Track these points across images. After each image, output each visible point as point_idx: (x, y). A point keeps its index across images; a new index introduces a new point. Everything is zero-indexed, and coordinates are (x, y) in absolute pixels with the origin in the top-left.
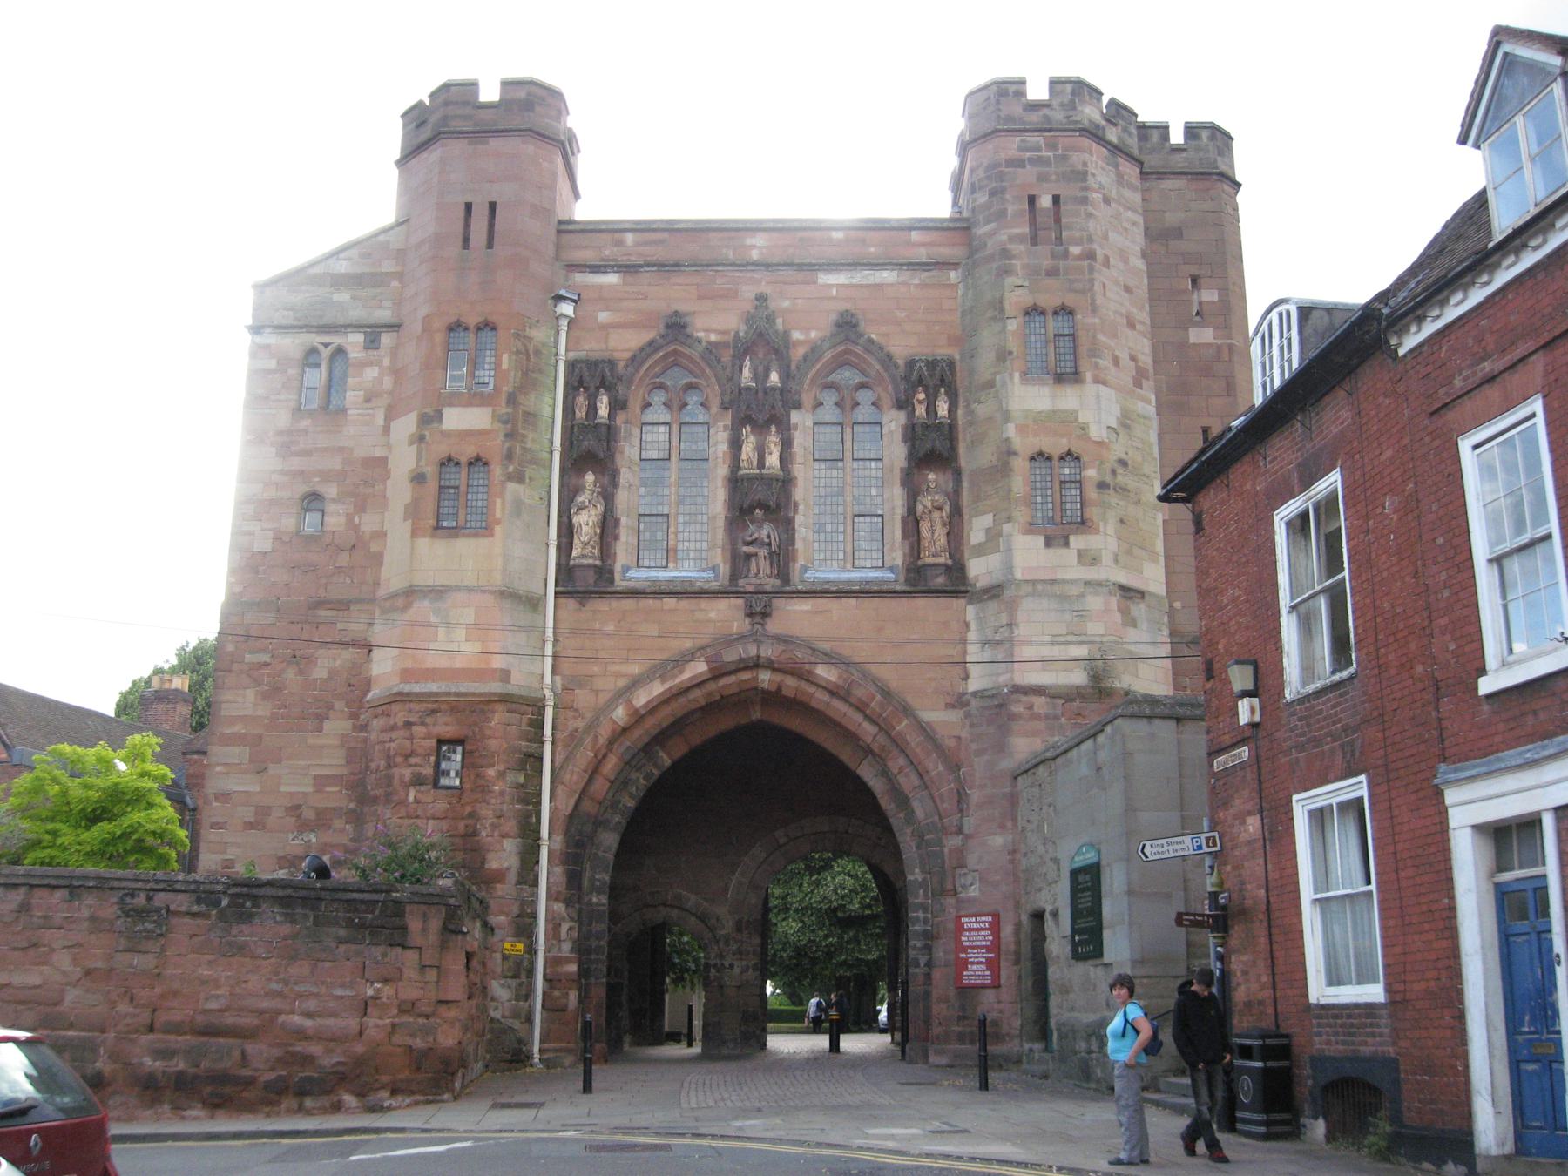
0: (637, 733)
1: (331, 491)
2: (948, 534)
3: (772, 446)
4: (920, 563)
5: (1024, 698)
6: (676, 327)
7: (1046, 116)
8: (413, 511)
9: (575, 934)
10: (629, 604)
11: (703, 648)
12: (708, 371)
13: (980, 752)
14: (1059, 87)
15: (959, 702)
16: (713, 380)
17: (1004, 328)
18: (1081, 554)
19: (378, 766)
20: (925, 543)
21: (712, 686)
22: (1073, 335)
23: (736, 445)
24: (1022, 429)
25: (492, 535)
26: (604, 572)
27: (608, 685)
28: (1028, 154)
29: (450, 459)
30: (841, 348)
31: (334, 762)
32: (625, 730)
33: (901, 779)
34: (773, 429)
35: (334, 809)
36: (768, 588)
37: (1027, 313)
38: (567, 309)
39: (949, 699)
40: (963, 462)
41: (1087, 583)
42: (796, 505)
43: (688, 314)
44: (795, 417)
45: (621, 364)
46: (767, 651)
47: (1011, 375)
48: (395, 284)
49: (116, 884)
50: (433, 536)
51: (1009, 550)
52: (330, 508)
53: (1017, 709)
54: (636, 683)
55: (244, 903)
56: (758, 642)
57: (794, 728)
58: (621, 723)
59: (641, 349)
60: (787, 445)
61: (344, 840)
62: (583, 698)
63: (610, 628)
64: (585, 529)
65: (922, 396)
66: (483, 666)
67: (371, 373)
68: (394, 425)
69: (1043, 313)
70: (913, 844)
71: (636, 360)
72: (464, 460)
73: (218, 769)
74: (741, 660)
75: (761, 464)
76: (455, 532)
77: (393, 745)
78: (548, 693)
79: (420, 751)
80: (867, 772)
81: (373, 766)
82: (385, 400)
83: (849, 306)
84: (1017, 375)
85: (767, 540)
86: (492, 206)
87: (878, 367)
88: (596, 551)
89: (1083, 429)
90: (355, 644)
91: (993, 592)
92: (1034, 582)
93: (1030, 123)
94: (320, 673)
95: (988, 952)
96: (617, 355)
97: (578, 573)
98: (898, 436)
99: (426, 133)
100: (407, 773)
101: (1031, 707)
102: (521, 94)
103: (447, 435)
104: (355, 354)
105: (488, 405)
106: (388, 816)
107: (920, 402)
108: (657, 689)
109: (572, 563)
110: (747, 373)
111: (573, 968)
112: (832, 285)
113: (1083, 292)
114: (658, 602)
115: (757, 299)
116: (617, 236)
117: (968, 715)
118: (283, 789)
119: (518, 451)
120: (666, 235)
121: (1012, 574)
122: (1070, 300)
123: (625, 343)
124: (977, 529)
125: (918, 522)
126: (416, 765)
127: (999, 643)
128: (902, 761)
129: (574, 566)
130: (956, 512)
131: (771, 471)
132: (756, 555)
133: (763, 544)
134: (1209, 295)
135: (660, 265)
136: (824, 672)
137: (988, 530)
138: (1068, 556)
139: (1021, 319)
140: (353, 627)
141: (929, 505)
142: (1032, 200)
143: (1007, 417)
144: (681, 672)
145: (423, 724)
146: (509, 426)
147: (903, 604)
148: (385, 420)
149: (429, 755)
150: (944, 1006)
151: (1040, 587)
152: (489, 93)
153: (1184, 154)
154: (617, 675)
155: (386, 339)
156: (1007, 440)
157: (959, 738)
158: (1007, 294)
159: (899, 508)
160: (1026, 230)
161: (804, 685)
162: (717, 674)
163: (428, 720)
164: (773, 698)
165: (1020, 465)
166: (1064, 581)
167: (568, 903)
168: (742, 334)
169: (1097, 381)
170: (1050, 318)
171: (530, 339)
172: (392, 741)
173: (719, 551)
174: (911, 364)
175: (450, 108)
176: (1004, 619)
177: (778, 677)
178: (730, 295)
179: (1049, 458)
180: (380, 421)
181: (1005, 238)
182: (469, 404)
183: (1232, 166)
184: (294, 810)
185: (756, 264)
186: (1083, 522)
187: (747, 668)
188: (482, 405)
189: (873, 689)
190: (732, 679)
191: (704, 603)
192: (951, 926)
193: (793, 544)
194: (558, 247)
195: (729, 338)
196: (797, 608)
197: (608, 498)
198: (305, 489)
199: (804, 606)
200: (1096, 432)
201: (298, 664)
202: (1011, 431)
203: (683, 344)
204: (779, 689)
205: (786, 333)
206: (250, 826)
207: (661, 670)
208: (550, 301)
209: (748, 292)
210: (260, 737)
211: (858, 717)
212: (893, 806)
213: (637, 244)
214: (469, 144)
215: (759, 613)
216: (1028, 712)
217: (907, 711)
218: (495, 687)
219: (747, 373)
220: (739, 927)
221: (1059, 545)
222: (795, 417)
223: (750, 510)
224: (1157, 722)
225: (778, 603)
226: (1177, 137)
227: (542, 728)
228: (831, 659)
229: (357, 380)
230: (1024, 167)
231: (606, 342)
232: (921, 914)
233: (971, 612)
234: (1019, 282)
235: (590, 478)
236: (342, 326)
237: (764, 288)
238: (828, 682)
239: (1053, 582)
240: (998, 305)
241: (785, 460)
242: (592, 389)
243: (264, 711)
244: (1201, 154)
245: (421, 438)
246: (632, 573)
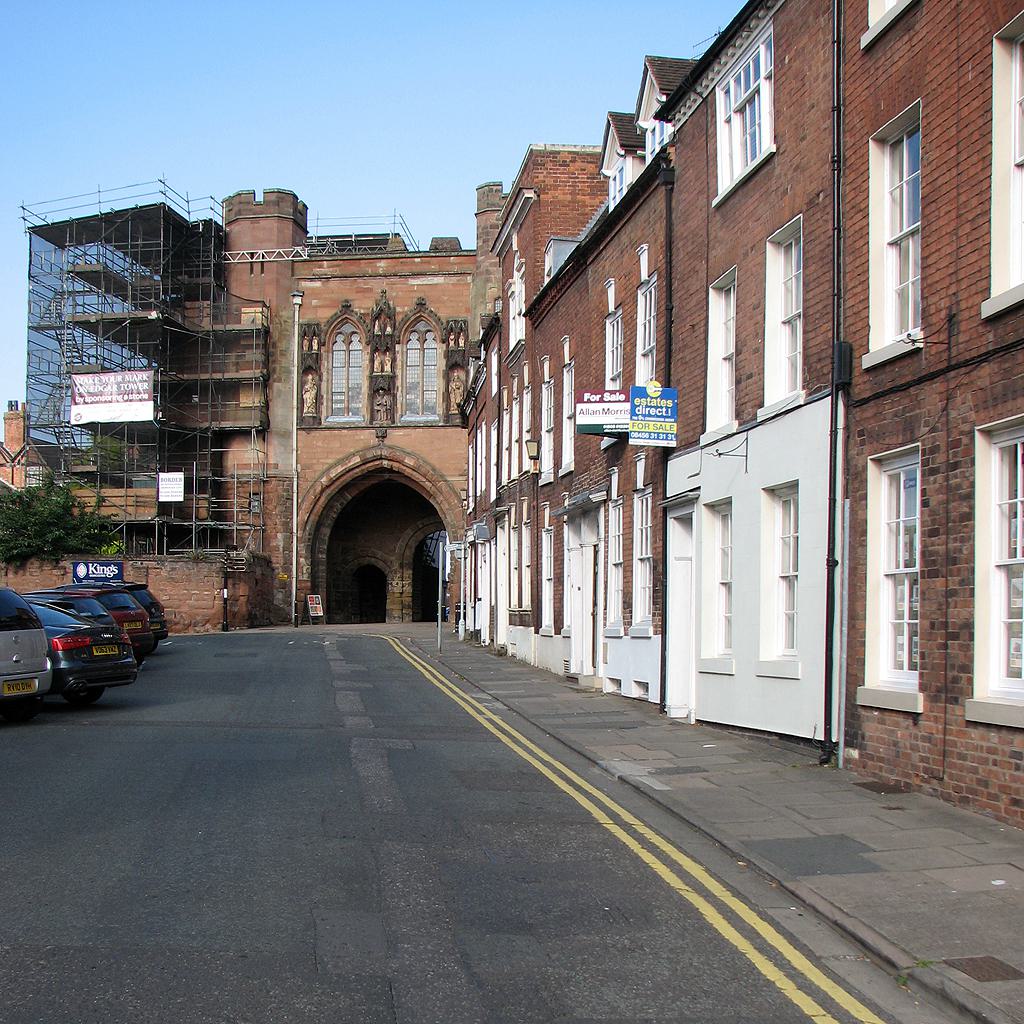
0: (332, 487)
6: (347, 307)
9: (310, 571)
21: (363, 467)
26: (317, 419)
27: (320, 468)
32: (328, 487)
38: (298, 300)
46: (385, 453)
60: (394, 360)
63: (320, 444)
71: (329, 323)
75: (382, 371)
83: (422, 295)
102: (273, 197)
108: (340, 469)
111: (309, 584)
123: (325, 315)
136: (409, 461)
154: (323, 464)
159: (442, 390)
164: (391, 470)
167: (306, 558)
171: (281, 317)
177: (391, 463)
191: (358, 432)
199: (401, 432)
205: (395, 308)
220: (401, 566)
223: (378, 390)
235: (310, 377)
241: (393, 367)
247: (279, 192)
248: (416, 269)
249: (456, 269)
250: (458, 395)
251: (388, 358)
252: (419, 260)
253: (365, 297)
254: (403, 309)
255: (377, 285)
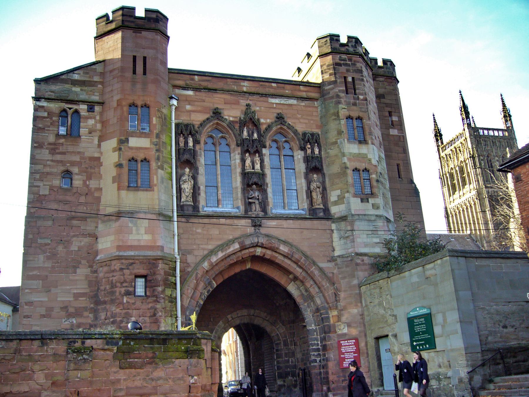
1: (75, 170)
2: (322, 197)
3: (257, 161)
4: (313, 208)
5: (360, 257)
6: (217, 113)
7: (347, 49)
8: (117, 179)
10: (206, 221)
11: (237, 239)
12: (230, 131)
13: (344, 278)
14: (351, 40)
15: (333, 259)
16: (233, 135)
17: (340, 123)
18: (373, 205)
19: (106, 288)
20: (314, 200)
21: (239, 254)
22: (362, 127)
23: (243, 161)
24: (349, 159)
25: (153, 191)
26: (196, 207)
27: (201, 253)
28: (342, 62)
29: (133, 159)
30: (279, 127)
31: (82, 287)
33: (311, 290)
34: (257, 155)
35: (84, 307)
36: (260, 215)
37: (347, 118)
38: (175, 102)
39: (329, 259)
40: (325, 172)
41: (377, 216)
42: (267, 184)
43: (221, 109)
44: (264, 151)
45: (196, 127)
46: (262, 240)
47: (344, 140)
48: (100, 86)
49: (66, 337)
50: (128, 190)
51: (349, 203)
52: (75, 177)
53: (359, 261)
54: (212, 252)
55: (130, 343)
56: (258, 237)
57: (263, 271)
58: (206, 269)
59: (204, 121)
60: (262, 162)
61: (90, 321)
62: (191, 259)
63: (199, 231)
64: (187, 190)
65: (309, 146)
66: (153, 245)
67: (91, 122)
68: (102, 144)
69: (352, 119)
70: (311, 315)
71: (202, 124)
72: (139, 159)
73: (27, 291)
74: (252, 243)
75: (253, 168)
76: (137, 188)
77: (114, 278)
78: (177, 256)
79: (128, 280)
80: (292, 288)
81: (102, 288)
82: (98, 134)
84: (346, 140)
85: (258, 197)
86: (145, 58)
87: (293, 134)
88: (191, 199)
89: (370, 160)
90: (90, 235)
91: (343, 218)
92: (358, 215)
93: (343, 51)
94: (74, 247)
95: (354, 354)
96: (194, 123)
97: (185, 208)
98: (302, 161)
99: (113, 26)
100: (123, 290)
101: (363, 261)
102: (154, 16)
103: (131, 148)
104: (83, 113)
105: (148, 137)
106: (113, 309)
107: (309, 148)
108: (220, 255)
109: (182, 204)
110: (245, 133)
112: (274, 103)
113: (365, 112)
114: (218, 220)
115: (247, 106)
116: (192, 76)
117: (336, 264)
118: (59, 299)
119: (161, 157)
120: (210, 78)
121: (351, 212)
122: (361, 114)
123: (197, 118)
124: (333, 196)
125: (311, 192)
126: (126, 287)
127: (348, 237)
128: (312, 282)
129: (183, 205)
130: (324, 189)
131: (258, 171)
132: (254, 203)
133: (256, 199)
134: (395, 118)
135: (210, 90)
136: (283, 248)
137: (338, 196)
138: (369, 206)
139: (345, 120)
140: (88, 228)
141: (315, 186)
142: (345, 78)
143: (344, 155)
144: (229, 248)
145: (128, 269)
146: (158, 146)
147: (308, 224)
148: (98, 142)
149: (132, 282)
150: (335, 376)
151: (361, 217)
152: (140, 13)
153: (383, 69)
154: (204, 249)
155: (97, 108)
156: (345, 163)
157: (333, 273)
158: (340, 111)
159: (305, 188)
160: (344, 88)
161: (274, 254)
162: (243, 248)
163: (130, 267)
165: (349, 172)
166: (368, 215)
168: (242, 119)
169: (373, 144)
170: (355, 120)
172: (113, 276)
173: (240, 201)
174: (304, 134)
175: (125, 17)
176: (349, 228)
177: (264, 250)
178: (238, 103)
179: (359, 171)
180: (96, 141)
181: (337, 90)
182: (140, 137)
183: (396, 75)
184: (65, 308)
185: (245, 92)
186: (372, 194)
187: (253, 247)
188: (145, 137)
189: (301, 255)
190: (247, 251)
192: (336, 345)
193: (267, 199)
194: (169, 79)
195: (238, 120)
196: (271, 223)
197: (194, 178)
198: (63, 168)
199: (273, 223)
200: (374, 162)
201: (64, 244)
202: (345, 160)
203: (219, 120)
204: (264, 255)
205: (258, 120)
206: (43, 316)
207: (222, 247)
208: (168, 99)
209: (243, 102)
210: (47, 276)
211: (295, 266)
212: (302, 301)
213: (199, 81)
214: (133, 32)
215: (257, 225)
216: (361, 263)
217: (314, 263)
218: (159, 253)
219: (245, 133)
221: (365, 202)
222: (264, 151)
223: (252, 184)
224: (460, 258)
225: (264, 221)
226: (380, 63)
227: (175, 271)
228: (285, 242)
229: (85, 124)
230: (341, 66)
231: (190, 118)
232: (316, 342)
233: (334, 226)
234: (344, 107)
236: (77, 101)
237: (251, 103)
238: (284, 252)
239: (365, 215)
240: (337, 114)
242: (186, 135)
243: (48, 264)
244: (388, 70)
245: (120, 149)
246: (205, 209)
247: (157, 12)
248: (272, 91)
249: (304, 95)
250: (319, 193)
251: (257, 159)
252: (274, 85)
253: (233, 109)
254: (265, 121)
255: (243, 102)
